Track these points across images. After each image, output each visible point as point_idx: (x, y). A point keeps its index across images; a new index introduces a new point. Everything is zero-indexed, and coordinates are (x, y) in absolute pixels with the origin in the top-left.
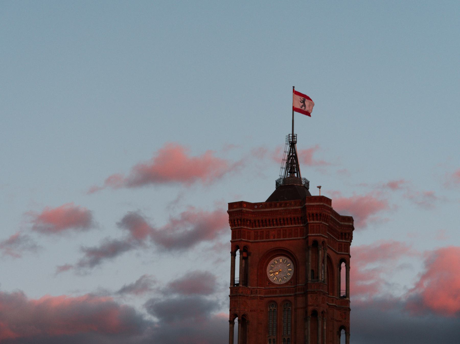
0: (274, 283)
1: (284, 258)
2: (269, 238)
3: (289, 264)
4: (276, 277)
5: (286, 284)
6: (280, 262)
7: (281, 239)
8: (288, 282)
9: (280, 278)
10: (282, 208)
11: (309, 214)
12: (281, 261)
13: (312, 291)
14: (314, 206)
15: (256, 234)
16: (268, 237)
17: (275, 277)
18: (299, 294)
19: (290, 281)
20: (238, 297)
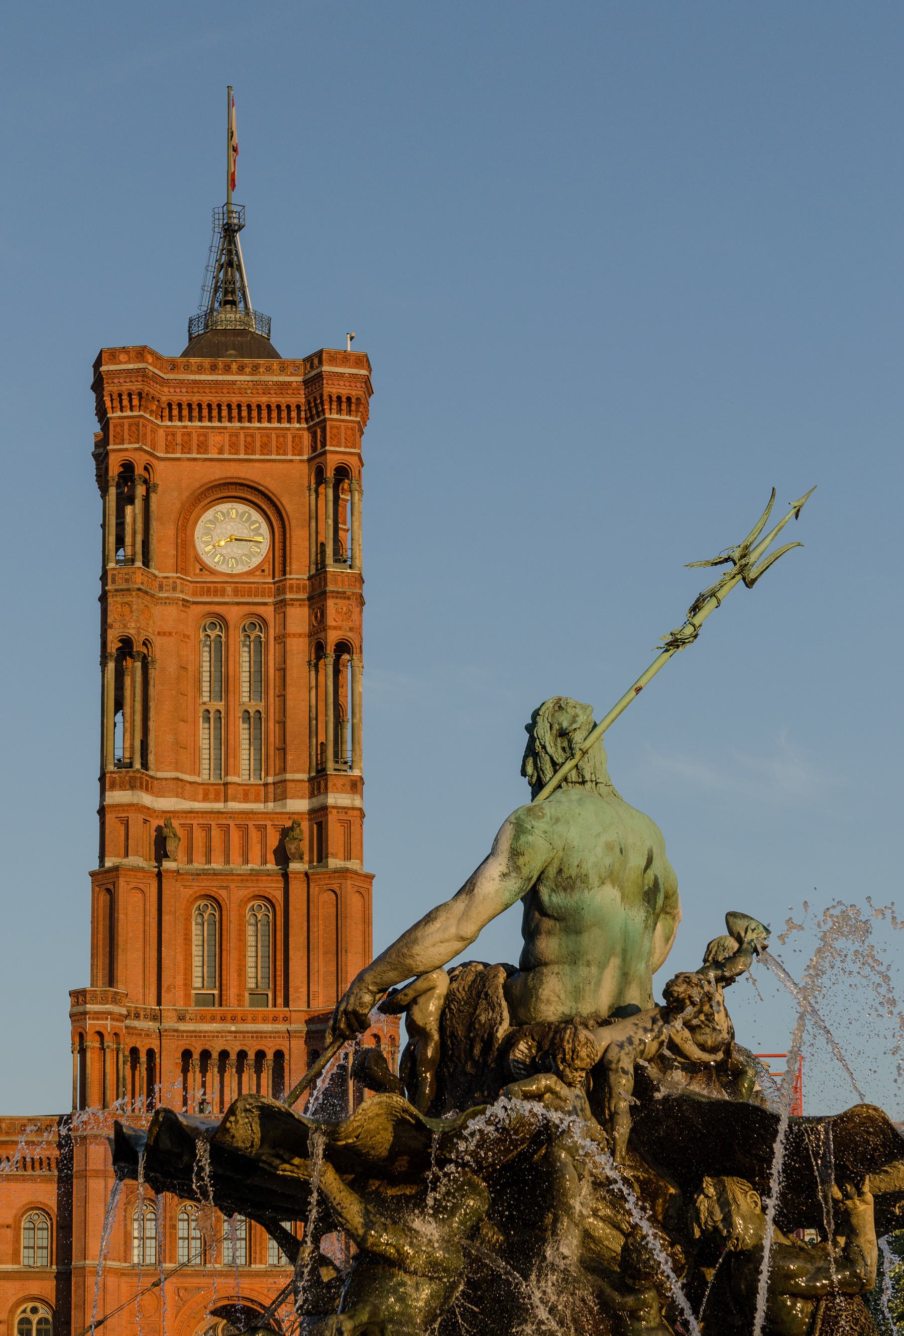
0: (216, 568)
1: (242, 508)
2: (206, 451)
3: (257, 525)
4: (222, 555)
5: (250, 573)
6: (231, 518)
7: (242, 456)
8: (252, 569)
9: (232, 558)
10: (248, 378)
11: (330, 397)
12: (233, 514)
13: (338, 592)
14: (342, 375)
15: (169, 437)
16: (203, 447)
17: (219, 556)
18: (292, 600)
19: (260, 568)
20: (134, 593)
